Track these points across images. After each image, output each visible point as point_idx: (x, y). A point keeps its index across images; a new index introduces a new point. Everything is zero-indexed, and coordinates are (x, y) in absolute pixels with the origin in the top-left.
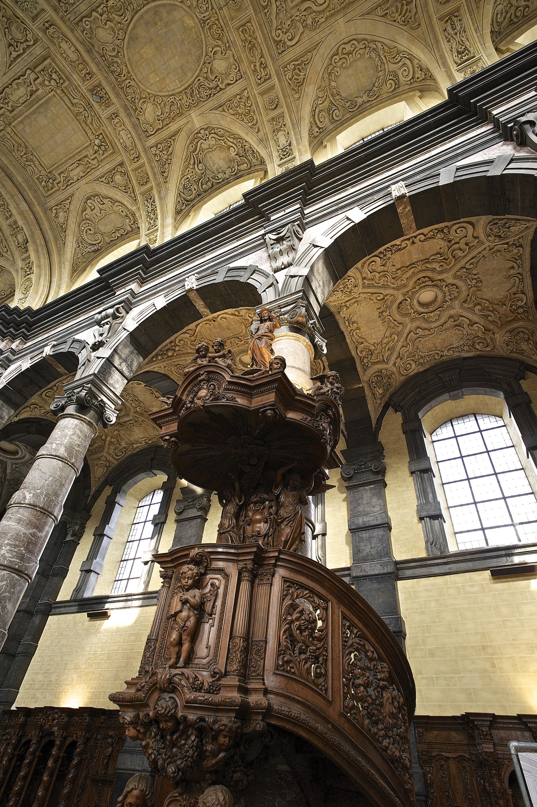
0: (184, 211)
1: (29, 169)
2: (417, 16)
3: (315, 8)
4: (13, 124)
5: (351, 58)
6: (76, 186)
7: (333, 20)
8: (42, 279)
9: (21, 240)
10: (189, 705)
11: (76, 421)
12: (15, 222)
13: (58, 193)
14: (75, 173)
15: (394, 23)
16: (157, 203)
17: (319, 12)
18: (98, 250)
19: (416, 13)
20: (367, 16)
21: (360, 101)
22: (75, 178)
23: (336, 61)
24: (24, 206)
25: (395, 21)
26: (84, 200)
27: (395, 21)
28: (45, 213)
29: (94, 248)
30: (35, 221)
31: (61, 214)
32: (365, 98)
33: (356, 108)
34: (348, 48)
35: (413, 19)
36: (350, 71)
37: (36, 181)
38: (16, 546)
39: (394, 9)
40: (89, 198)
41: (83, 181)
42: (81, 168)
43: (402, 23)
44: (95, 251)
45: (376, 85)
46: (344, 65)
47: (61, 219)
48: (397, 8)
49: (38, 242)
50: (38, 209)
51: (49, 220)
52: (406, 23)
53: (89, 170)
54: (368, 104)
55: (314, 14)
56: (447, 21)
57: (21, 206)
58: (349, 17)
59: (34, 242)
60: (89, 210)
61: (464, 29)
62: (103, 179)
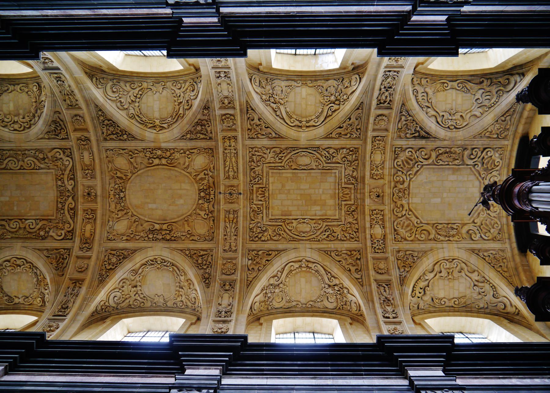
2: (65, 269)
3: (8, 228)
5: (19, 269)
7: (15, 241)
15: (50, 265)
17: (10, 232)
19: (66, 267)
20: (37, 251)
21: (16, 300)
23: (6, 265)
25: (52, 264)
27: (52, 264)
32: (21, 300)
33: (11, 304)
34: (19, 262)
35: (62, 269)
36: (16, 277)
39: (54, 256)
43: (55, 268)
45: (31, 296)
46: (12, 271)
48: (56, 257)
52: (57, 269)
54: (22, 306)
55: (5, 230)
56: (73, 283)
58: (25, 244)
61: (78, 294)
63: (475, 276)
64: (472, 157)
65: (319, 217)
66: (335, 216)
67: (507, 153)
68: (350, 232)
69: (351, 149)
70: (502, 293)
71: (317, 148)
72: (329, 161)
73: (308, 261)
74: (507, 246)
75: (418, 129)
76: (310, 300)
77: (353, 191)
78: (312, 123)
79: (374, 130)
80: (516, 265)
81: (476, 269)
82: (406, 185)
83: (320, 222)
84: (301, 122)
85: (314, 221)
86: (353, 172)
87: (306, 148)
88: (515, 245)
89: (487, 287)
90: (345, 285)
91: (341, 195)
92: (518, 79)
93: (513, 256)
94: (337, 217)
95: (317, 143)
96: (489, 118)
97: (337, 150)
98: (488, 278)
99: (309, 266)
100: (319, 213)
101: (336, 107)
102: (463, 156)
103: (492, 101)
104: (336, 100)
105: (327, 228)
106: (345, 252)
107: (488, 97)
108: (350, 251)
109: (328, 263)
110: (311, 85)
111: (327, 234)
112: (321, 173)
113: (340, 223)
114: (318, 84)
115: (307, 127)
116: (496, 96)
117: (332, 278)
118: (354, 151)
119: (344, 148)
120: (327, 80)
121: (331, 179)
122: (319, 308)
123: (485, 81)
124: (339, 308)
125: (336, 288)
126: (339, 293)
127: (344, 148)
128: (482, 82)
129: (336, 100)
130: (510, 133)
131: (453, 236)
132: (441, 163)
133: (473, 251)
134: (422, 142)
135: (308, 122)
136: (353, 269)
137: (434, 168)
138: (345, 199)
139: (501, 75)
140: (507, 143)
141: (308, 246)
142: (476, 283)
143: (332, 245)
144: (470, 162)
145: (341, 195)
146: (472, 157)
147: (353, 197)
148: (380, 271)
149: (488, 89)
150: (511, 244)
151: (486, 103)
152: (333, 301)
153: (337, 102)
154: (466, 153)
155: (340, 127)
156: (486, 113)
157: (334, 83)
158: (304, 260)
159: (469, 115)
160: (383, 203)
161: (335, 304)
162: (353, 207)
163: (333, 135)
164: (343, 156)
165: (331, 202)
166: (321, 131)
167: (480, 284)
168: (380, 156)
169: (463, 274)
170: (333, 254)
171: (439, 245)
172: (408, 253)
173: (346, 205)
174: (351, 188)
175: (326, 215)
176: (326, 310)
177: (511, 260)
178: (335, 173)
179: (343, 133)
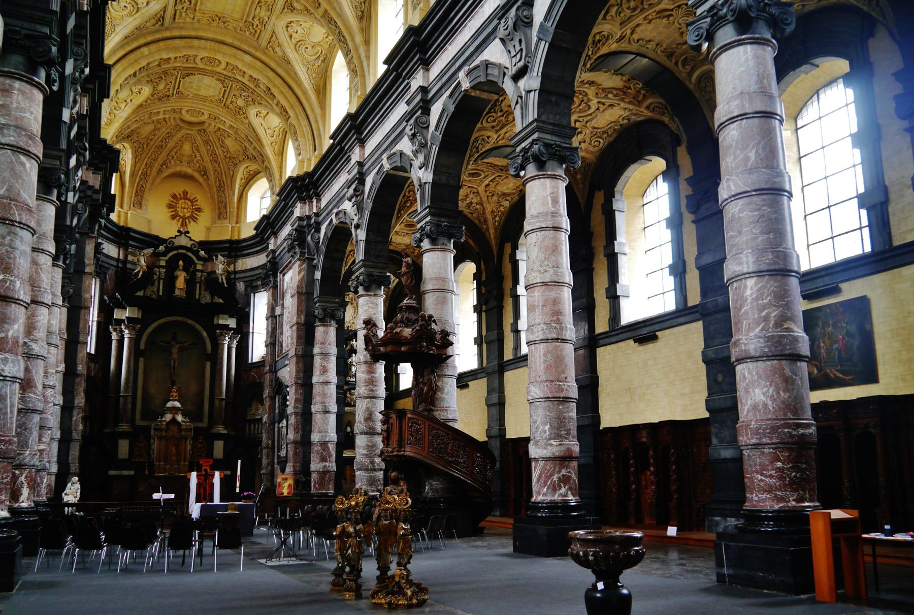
0: (366, 10)
1: (230, 27)
4: (198, 8)
6: (271, 24)
8: (300, 118)
9: (265, 89)
10: (387, 456)
11: (367, 298)
12: (251, 76)
13: (263, 33)
14: (263, 13)
16: (339, 24)
18: (325, 59)
22: (266, 19)
24: (248, 58)
26: (285, 30)
28: (265, 54)
29: (320, 61)
30: (263, 66)
31: (277, 49)
37: (241, 32)
38: (367, 386)
40: (287, 27)
41: (273, 18)
42: (264, 8)
44: (323, 61)
47: (280, 54)
49: (276, 82)
50: (258, 54)
51: (271, 58)
53: (270, 7)
57: (245, 60)
59: (275, 85)
60: (294, 35)
62: (286, 9)
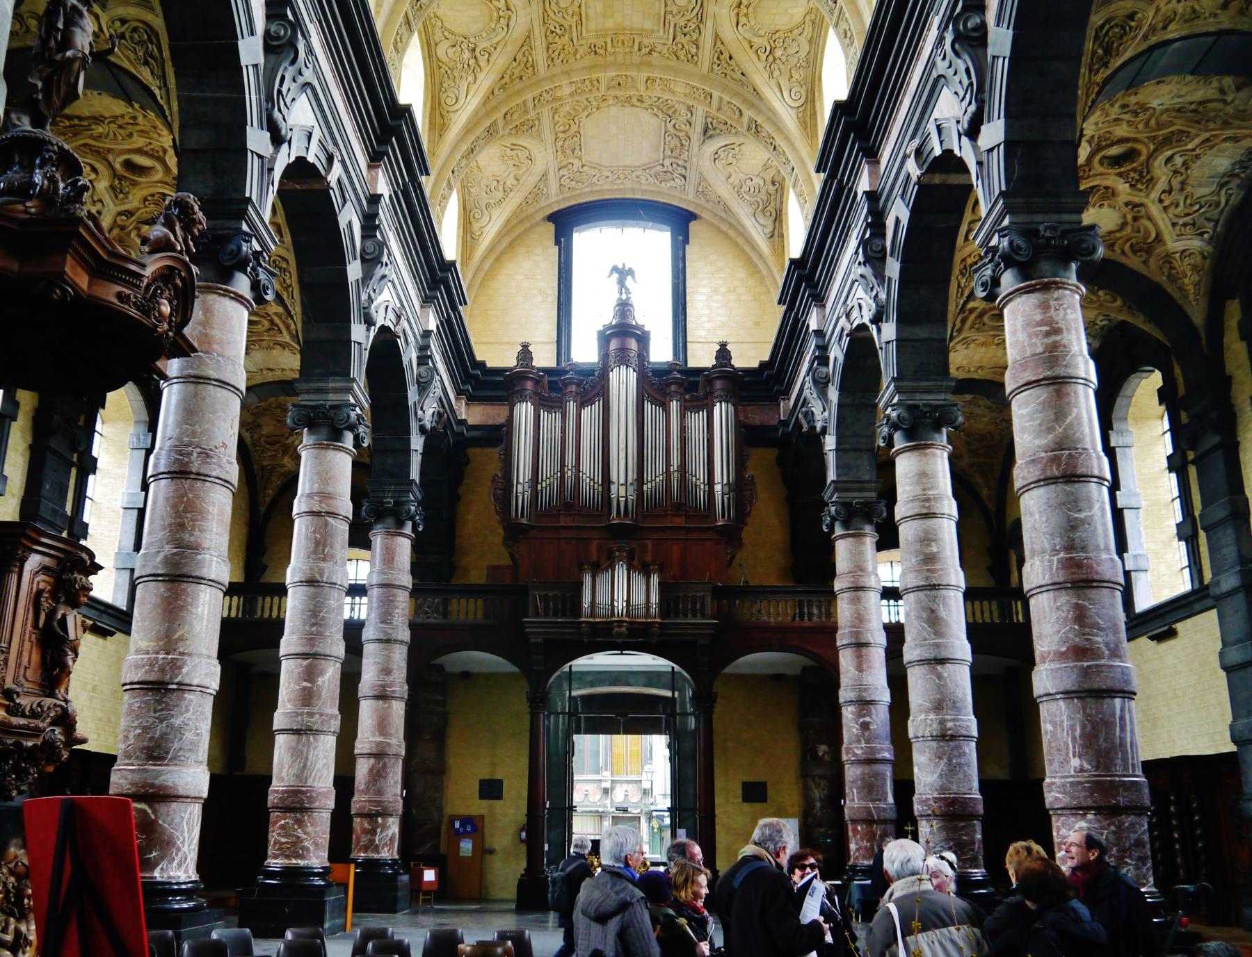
63: (510, 182)
64: (675, 166)
65: (583, 14)
66: (587, 31)
67: (677, 194)
68: (562, 55)
69: (696, 58)
70: (495, 213)
71: (701, 18)
72: (679, 30)
73: (509, 19)
74: (554, 199)
75: (718, 131)
76: (444, 19)
77: (627, 50)
78: (743, 20)
79: (721, 99)
80: (531, 215)
81: (521, 182)
82: (638, 104)
83: (576, 18)
84: (747, 7)
85: (577, 10)
86: (660, 53)
87: (702, 6)
88: (556, 208)
89: (499, 195)
90: (481, 76)
91: (622, 37)
92: (767, 231)
93: (542, 208)
94: (584, 34)
95: (709, 24)
96: (725, 192)
97: (696, 43)
98: (510, 196)
99: (502, 20)
100: (591, 12)
101: (763, 57)
102: (676, 158)
103: (745, 196)
104: (775, 59)
105: (567, 27)
106: (530, 59)
107: (752, 190)
108: (533, 66)
109: (511, 49)
110: (808, 18)
111: (558, 30)
112: (659, 15)
113: (575, 41)
114: (806, 30)
115: (738, 14)
116: (753, 200)
117: (487, 55)
118: (693, 58)
119: (698, 48)
120: (810, 42)
121: (648, 25)
122: (433, 34)
123: (775, 188)
124: (440, 67)
125: (472, 62)
126: (466, 66)
127: (698, 48)
128: (773, 183)
129: (775, 59)
130: (703, 202)
131: (563, 152)
132: (667, 139)
133: (545, 175)
134: (699, 128)
135: (746, 15)
136: (507, 79)
137: (661, 129)
138: (615, 42)
139: (778, 206)
140: (691, 197)
141: (535, 16)
142: (501, 183)
143: (539, 43)
144: (667, 162)
145: (622, 37)
146: (675, 166)
147: (617, 50)
148: (508, 116)
149: (763, 190)
150: (557, 202)
151: (745, 188)
152: (450, 55)
153: (771, 58)
154: (681, 163)
155: (731, 58)
156: (731, 190)
157: (803, 54)
158: (509, 12)
159: (731, 171)
160: (609, 88)
161: (445, 59)
162: (601, 52)
163: (719, 42)
164: (686, 45)
165: (610, 24)
166: (728, 33)
167: (501, 188)
168: (683, 91)
169: (512, 169)
170: (525, 48)
171: (549, 146)
172: (537, 122)
173: (606, 43)
174: (633, 46)
175: (587, 20)
176: (433, 44)
177: (538, 207)
178: (658, 31)
179: (722, 57)
